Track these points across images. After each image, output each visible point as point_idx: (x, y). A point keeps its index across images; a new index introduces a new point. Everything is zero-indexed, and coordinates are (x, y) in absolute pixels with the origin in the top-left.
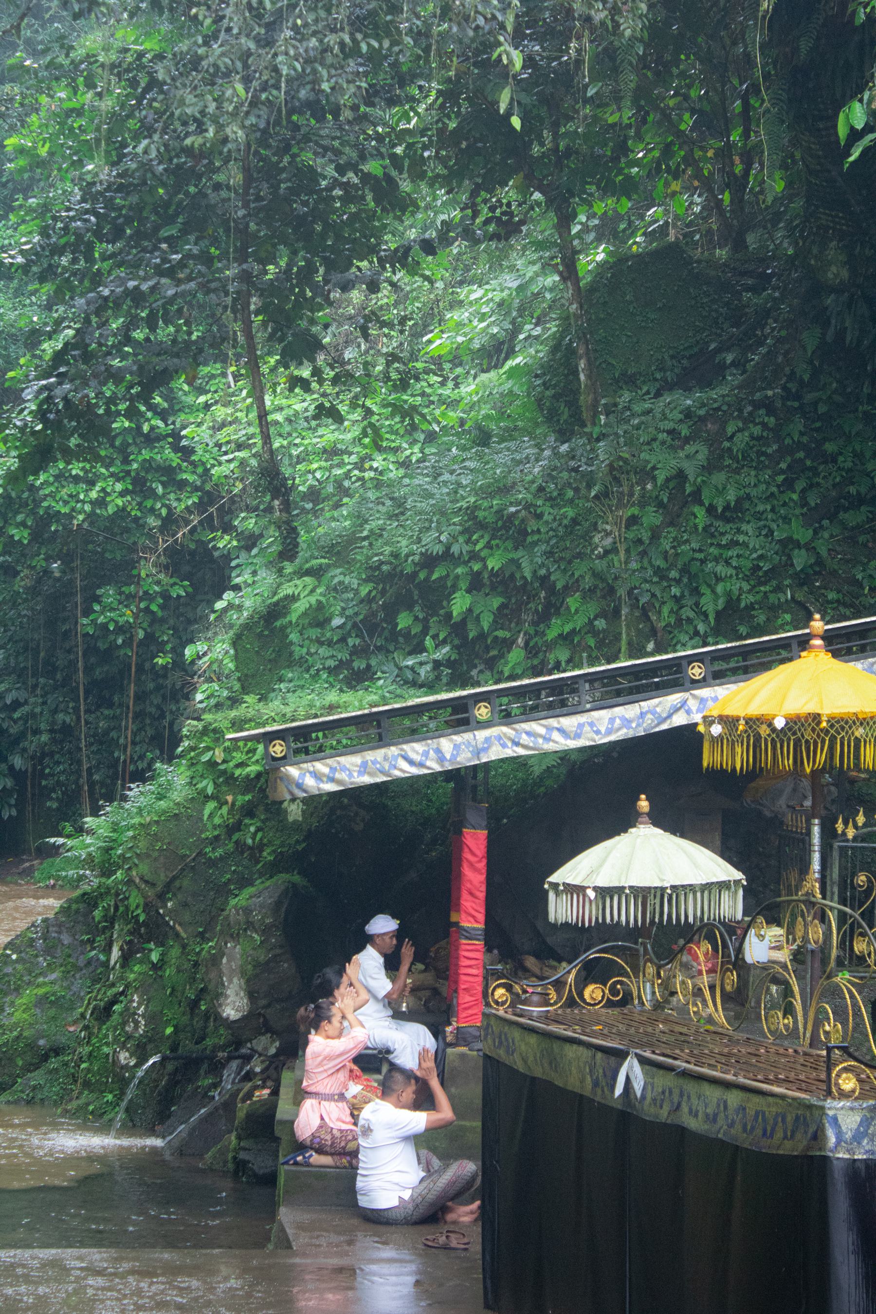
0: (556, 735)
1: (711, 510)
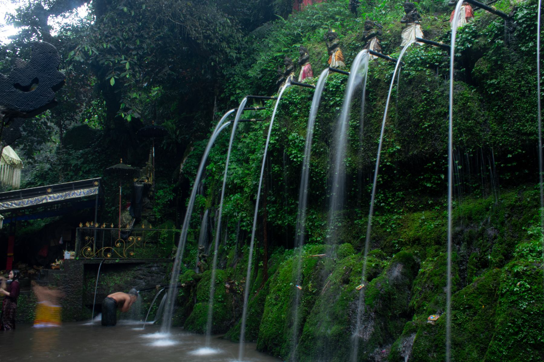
0: (14, 205)
1: (83, 171)
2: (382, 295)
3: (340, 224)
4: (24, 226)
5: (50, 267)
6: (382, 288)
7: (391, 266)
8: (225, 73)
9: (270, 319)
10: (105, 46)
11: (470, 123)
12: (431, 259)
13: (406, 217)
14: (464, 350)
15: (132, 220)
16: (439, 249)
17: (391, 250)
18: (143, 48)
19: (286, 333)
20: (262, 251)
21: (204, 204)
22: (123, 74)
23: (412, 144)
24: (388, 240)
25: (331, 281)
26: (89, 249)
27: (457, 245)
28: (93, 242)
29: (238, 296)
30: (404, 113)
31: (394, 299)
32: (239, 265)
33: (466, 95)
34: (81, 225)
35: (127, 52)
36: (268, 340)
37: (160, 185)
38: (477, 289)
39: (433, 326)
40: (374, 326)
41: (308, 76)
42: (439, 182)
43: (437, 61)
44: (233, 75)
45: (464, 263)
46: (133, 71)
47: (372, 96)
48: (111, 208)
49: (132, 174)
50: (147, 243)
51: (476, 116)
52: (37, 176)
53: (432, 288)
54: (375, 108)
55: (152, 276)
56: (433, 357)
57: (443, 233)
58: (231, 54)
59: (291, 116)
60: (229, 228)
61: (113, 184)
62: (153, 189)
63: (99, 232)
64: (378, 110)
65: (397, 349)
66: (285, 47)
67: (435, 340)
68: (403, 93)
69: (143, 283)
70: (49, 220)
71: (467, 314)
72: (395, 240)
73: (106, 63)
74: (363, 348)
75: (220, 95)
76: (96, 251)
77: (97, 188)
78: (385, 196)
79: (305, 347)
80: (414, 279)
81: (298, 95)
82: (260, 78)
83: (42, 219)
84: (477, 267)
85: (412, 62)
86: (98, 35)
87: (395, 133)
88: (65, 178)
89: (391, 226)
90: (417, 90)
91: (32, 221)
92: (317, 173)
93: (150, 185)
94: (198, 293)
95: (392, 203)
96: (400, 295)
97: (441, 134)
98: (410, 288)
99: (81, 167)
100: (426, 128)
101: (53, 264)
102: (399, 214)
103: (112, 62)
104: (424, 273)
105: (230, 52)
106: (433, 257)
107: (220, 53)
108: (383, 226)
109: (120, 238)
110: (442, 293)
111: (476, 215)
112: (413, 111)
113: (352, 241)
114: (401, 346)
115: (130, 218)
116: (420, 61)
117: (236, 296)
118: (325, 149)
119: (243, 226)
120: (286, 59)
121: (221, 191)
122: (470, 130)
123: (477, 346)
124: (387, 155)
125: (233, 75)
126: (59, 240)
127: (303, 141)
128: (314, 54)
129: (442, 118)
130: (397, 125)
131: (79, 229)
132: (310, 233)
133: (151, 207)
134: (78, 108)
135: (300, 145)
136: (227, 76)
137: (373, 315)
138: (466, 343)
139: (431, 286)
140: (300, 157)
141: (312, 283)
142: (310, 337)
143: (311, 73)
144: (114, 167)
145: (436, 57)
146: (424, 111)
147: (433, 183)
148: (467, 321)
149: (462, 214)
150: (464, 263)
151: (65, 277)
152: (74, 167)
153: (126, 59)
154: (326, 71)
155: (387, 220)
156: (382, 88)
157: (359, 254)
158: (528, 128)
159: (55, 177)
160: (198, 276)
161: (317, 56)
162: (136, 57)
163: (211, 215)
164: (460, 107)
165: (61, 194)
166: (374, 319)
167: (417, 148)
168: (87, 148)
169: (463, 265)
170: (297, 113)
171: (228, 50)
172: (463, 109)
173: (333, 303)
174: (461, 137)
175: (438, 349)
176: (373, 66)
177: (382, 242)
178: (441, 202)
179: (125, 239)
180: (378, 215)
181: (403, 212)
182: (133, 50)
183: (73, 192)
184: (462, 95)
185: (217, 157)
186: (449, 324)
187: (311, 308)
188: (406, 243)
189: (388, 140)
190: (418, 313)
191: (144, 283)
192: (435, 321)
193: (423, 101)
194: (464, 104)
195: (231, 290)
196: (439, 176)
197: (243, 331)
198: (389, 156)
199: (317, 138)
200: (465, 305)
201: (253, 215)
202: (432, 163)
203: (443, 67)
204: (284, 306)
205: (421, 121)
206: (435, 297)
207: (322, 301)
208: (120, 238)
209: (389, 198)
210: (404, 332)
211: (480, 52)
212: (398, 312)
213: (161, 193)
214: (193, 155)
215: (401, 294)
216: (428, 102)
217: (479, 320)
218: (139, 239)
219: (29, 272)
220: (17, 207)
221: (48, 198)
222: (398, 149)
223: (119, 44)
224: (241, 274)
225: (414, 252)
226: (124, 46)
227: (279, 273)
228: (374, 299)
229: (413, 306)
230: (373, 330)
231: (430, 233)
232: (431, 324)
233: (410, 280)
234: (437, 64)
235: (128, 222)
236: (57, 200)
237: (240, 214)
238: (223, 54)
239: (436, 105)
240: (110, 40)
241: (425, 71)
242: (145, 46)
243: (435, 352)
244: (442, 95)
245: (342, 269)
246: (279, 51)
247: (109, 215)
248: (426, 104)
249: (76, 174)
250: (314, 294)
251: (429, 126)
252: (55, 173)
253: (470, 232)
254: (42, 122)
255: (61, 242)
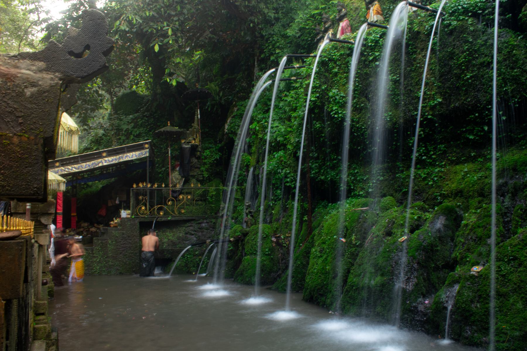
0: (74, 169)
1: (134, 135)
2: (424, 246)
3: (382, 178)
4: (84, 188)
5: (109, 225)
6: (424, 240)
7: (434, 218)
8: (264, 34)
9: (315, 271)
10: (148, 14)
11: (515, 72)
12: (474, 211)
13: (448, 170)
14: (509, 300)
15: (181, 179)
16: (482, 201)
17: (432, 202)
18: (184, 14)
19: (331, 283)
20: (306, 206)
21: (249, 162)
22: (166, 41)
23: (454, 96)
24: (430, 193)
25: (374, 234)
26: (143, 208)
27: (501, 197)
28: (146, 201)
29: (284, 249)
30: (445, 65)
31: (437, 251)
32: (284, 219)
33: (512, 43)
34: (135, 186)
35: (168, 18)
36: (314, 291)
37: (207, 145)
38: (523, 240)
39: (477, 277)
40: (417, 277)
41: (346, 32)
42: (482, 134)
43: (480, 9)
44: (272, 35)
45: (508, 215)
46: (176, 37)
47: (411, 49)
48: (161, 168)
49: (179, 136)
50: (196, 201)
51: (523, 64)
52: (92, 142)
53: (475, 240)
54: (415, 61)
55: (202, 232)
56: (476, 307)
57: (486, 185)
58: (270, 14)
59: (330, 73)
60: (274, 185)
61: (162, 146)
62: (200, 150)
63: (152, 191)
64: (418, 63)
65: (440, 299)
66: (322, 4)
67: (478, 290)
68: (444, 45)
69: (194, 239)
70: (105, 182)
71: (512, 266)
72: (437, 193)
73: (149, 31)
74: (406, 298)
75: (260, 56)
76: (150, 209)
77: (148, 150)
78: (427, 149)
79: (349, 297)
80: (457, 231)
81: (337, 52)
82: (299, 37)
83: (100, 181)
84: (522, 218)
85: (454, 12)
86: (140, 3)
87: (436, 86)
88: (118, 142)
89: (433, 179)
90: (459, 41)
91: (90, 183)
92: (358, 128)
93: (197, 146)
94: (246, 247)
95: (433, 157)
96: (443, 247)
97: (484, 85)
98: (452, 240)
99: (132, 132)
100: (468, 79)
101: (112, 223)
102: (441, 166)
103: (155, 29)
104: (466, 225)
105: (268, 13)
106: (476, 209)
107: (258, 14)
108: (425, 179)
109: (170, 197)
110: (485, 244)
111: (521, 166)
112: (455, 63)
113: (394, 194)
114: (444, 296)
115: (180, 177)
116: (462, 10)
117: (282, 249)
118: (365, 104)
119: (287, 182)
120: (324, 16)
121: (265, 149)
122: (515, 80)
123: (523, 297)
124: (428, 109)
125: (272, 35)
126: (115, 200)
127: (343, 97)
128: (351, 9)
129: (485, 68)
130: (438, 78)
131: (133, 190)
132: (352, 187)
133: (199, 166)
134: (126, 75)
135: (341, 101)
136: (267, 37)
137: (415, 266)
138: (511, 294)
139: (474, 238)
140: (341, 113)
141: (356, 235)
142: (354, 288)
143: (349, 28)
144: (162, 130)
145: (479, 4)
146: (467, 62)
147: (476, 135)
148: (511, 272)
149: (506, 166)
150: (508, 215)
151: (123, 234)
152: (125, 131)
153: (168, 25)
154: (364, 26)
155: (429, 173)
156: (422, 41)
157: (401, 207)
159: (108, 142)
160: (246, 231)
161: (355, 11)
162: (177, 23)
163: (256, 173)
164: (505, 55)
165: (115, 157)
166: (417, 270)
167: (459, 100)
168: (136, 113)
169: (508, 217)
170: (336, 70)
171: (266, 11)
172: (509, 57)
173: (376, 255)
174: (505, 87)
175: (482, 300)
176: (412, 18)
177: (424, 194)
178: (484, 154)
179: (176, 198)
180: (419, 169)
181: (445, 165)
182: (174, 16)
183: (125, 155)
184: (507, 43)
185: (259, 116)
186: (493, 276)
187: (355, 259)
188: (448, 196)
189: (428, 93)
190: (461, 264)
191: (195, 239)
192: (478, 272)
193: (465, 52)
194: (509, 52)
195: (277, 243)
196: (482, 128)
197: (289, 282)
198: (430, 109)
199: (357, 94)
200: (510, 256)
201: (296, 171)
202: (474, 115)
203: (487, 14)
204: (329, 258)
205: (463, 73)
206: (479, 249)
207: (366, 253)
208: (170, 197)
209: (430, 151)
210: (446, 283)
212: (440, 263)
213: (207, 152)
214: (237, 115)
215: (444, 246)
216: (471, 53)
217: (524, 271)
218: (189, 197)
219: (91, 230)
220: (77, 171)
221: (104, 161)
222: (439, 102)
223: (161, 11)
224: (286, 228)
225: (456, 204)
226: (165, 12)
227: (323, 227)
228: (417, 250)
229: (456, 257)
230: (416, 281)
231: (473, 185)
232: (474, 275)
233: (453, 232)
234: (480, 12)
235: (178, 181)
236: (112, 163)
237: (284, 171)
238: (261, 15)
239: (479, 55)
240: (152, 8)
241: (467, 20)
242: (185, 11)
243: (478, 302)
244: (485, 44)
245: (384, 222)
246: (317, 9)
247: (160, 175)
248: (468, 55)
249: (128, 138)
250: (357, 246)
251: (471, 77)
252: (108, 138)
253: (515, 183)
254: (94, 91)
255: (117, 202)
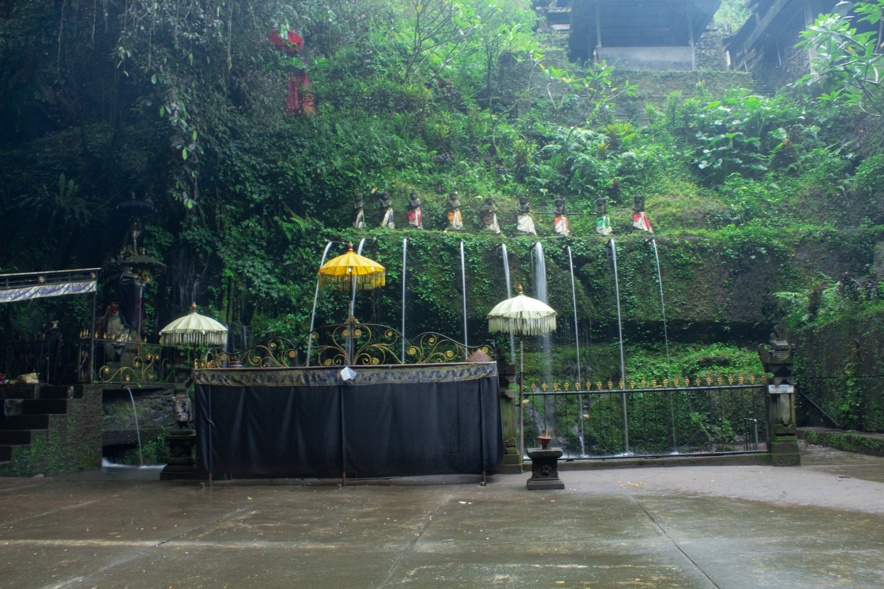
158: (614, 314)
211: (588, 260)
